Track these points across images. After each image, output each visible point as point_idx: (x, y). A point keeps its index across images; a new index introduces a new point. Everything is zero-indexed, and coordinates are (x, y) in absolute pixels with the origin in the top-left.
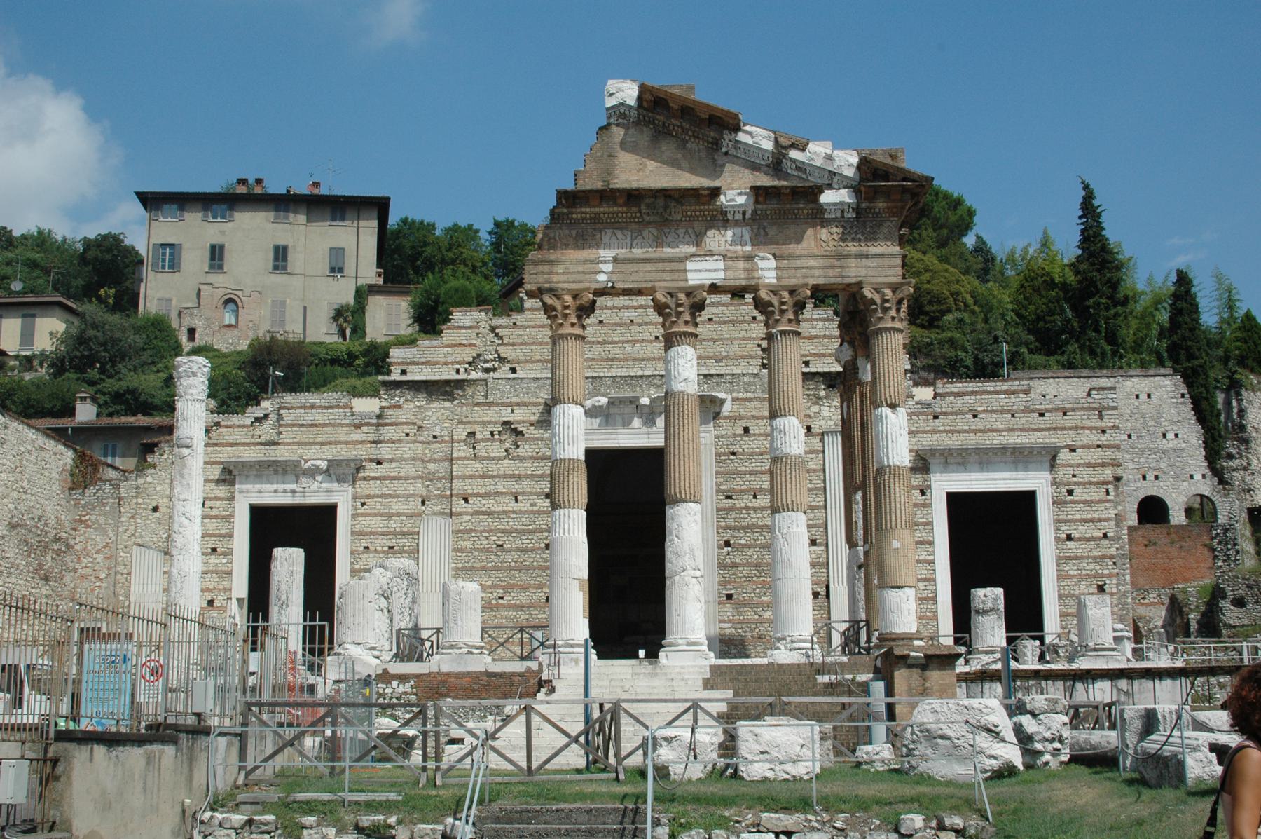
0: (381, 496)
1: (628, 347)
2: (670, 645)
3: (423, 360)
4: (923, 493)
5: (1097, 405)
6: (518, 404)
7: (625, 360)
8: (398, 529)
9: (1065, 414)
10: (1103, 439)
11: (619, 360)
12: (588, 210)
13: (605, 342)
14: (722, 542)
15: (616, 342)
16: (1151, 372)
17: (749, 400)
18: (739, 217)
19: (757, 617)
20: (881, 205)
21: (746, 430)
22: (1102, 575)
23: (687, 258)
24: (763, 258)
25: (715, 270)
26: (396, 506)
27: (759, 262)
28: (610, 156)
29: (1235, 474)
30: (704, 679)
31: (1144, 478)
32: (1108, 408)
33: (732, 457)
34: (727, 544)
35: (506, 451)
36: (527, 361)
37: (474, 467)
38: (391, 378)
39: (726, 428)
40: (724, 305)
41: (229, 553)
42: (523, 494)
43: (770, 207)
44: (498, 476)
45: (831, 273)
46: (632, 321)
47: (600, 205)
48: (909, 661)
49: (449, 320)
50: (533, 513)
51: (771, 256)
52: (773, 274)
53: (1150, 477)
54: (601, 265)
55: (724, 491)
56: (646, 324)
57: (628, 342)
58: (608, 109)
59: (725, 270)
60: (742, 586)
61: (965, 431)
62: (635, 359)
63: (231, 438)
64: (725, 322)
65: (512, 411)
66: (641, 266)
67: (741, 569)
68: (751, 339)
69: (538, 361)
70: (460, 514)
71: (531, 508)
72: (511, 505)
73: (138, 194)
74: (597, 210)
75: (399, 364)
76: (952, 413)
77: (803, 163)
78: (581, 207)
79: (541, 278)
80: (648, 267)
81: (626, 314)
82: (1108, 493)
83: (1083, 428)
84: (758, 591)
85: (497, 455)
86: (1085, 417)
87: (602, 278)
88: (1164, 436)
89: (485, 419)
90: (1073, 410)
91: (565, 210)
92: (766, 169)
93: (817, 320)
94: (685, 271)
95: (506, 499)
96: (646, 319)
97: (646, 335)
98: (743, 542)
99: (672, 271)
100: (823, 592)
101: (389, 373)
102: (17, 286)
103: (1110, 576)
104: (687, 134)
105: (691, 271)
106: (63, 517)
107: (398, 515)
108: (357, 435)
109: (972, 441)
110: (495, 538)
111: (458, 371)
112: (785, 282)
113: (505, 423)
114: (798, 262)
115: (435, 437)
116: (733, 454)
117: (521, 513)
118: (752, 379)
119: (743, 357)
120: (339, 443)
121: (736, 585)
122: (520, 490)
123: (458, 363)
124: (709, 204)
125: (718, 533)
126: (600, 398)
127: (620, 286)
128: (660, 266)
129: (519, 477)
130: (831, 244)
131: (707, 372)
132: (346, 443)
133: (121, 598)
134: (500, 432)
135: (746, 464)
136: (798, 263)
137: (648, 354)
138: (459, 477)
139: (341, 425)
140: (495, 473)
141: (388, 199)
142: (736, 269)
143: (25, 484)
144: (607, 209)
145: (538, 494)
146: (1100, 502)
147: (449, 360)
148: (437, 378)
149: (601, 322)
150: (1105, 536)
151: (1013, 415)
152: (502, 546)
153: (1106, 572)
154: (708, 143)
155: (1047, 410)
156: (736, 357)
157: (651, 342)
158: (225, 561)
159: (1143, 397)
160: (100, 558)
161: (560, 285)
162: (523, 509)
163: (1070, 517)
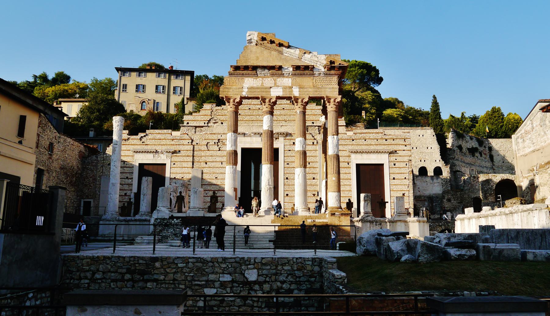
0: (180, 162)
3: (193, 120)
4: (348, 164)
7: (257, 121)
8: (185, 172)
9: (394, 140)
11: (255, 121)
12: (240, 72)
13: (250, 115)
14: (285, 178)
15: (254, 115)
16: (424, 128)
20: (333, 72)
22: (404, 191)
23: (270, 88)
25: (280, 92)
26: (185, 165)
29: (450, 160)
30: (272, 220)
31: (421, 161)
32: (407, 139)
34: (287, 178)
35: (219, 148)
37: (208, 153)
38: (184, 125)
39: (288, 142)
40: (288, 104)
41: (132, 178)
46: (259, 109)
49: (203, 107)
52: (298, 93)
53: (423, 161)
55: (286, 162)
57: (258, 115)
58: (248, 40)
61: (362, 145)
63: (133, 143)
64: (289, 110)
65: (221, 136)
66: (256, 90)
70: (204, 168)
72: (220, 165)
73: (115, 68)
74: (243, 72)
75: (187, 121)
76: (358, 139)
79: (225, 93)
80: (259, 90)
82: (406, 165)
83: (400, 145)
85: (216, 149)
88: (427, 148)
89: (213, 138)
91: (233, 72)
93: (317, 109)
94: (270, 92)
99: (266, 92)
100: (317, 194)
101: (183, 123)
102: (78, 96)
103: (407, 190)
106: (80, 166)
107: (185, 167)
108: (173, 143)
109: (364, 148)
111: (205, 123)
112: (301, 96)
113: (219, 140)
115: (197, 144)
120: (167, 145)
123: (205, 121)
127: (249, 96)
128: (263, 90)
132: (169, 145)
133: (97, 192)
138: (204, 156)
139: (168, 139)
141: (194, 72)
143: (66, 156)
146: (404, 167)
147: (202, 120)
148: (198, 125)
149: (250, 109)
150: (405, 178)
151: (377, 140)
153: (406, 189)
155: (389, 139)
158: (130, 181)
159: (421, 136)
160: (91, 179)
161: (231, 96)
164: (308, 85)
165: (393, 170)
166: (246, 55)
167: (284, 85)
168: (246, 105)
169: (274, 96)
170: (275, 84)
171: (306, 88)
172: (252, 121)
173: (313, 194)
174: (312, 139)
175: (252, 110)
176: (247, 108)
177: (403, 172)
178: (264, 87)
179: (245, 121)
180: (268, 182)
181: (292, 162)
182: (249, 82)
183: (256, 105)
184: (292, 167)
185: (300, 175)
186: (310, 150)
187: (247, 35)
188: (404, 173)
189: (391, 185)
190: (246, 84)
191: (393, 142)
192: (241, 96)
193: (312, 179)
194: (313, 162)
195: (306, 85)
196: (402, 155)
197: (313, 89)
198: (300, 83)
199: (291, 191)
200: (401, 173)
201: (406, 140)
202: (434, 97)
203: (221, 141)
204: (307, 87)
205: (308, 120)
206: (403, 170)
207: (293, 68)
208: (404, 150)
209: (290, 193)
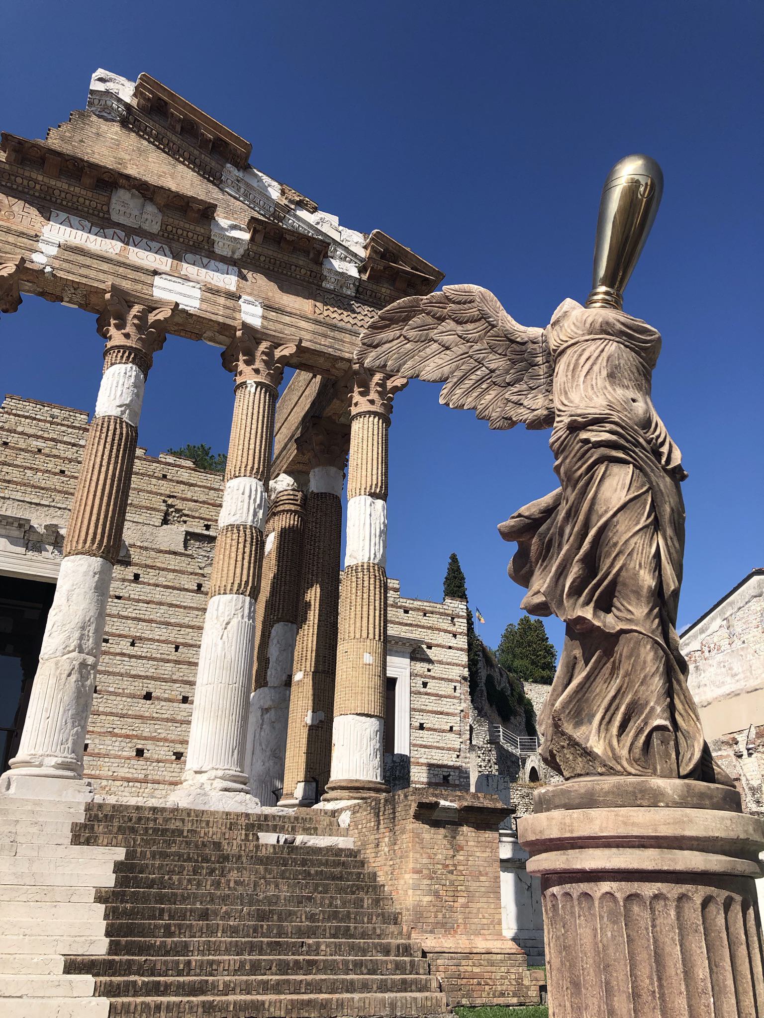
1: (29, 473)
2: (27, 763)
5: (450, 612)
7: (25, 485)
10: (455, 642)
11: (17, 483)
12: (40, 178)
17: (146, 549)
21: (137, 577)
23: (155, 273)
24: (249, 303)
28: (82, 141)
33: (116, 600)
43: (266, 251)
48: (436, 815)
56: (55, 456)
59: (202, 300)
62: (33, 486)
66: (95, 263)
68: (157, 494)
74: (53, 182)
80: (105, 266)
81: (35, 443)
82: (455, 689)
83: (439, 630)
86: (441, 620)
87: (39, 260)
90: (432, 613)
91: (7, 167)
94: (152, 285)
96: (55, 452)
97: (50, 466)
99: (135, 281)
105: (159, 288)
119: (148, 508)
128: (121, 270)
137: (49, 484)
142: (215, 303)
144: (65, 186)
155: (412, 609)
156: (141, 507)
157: (55, 474)
163: (423, 707)
165: (422, 702)
166: (77, 138)
173: (175, 754)
174: (196, 574)
175: (13, 448)
177: (446, 710)
178: (127, 262)
180: (77, 635)
181: (120, 636)
183: (29, 436)
184: (118, 651)
185: (234, 622)
186: (185, 608)
187: (95, 76)
188: (448, 714)
189: (415, 745)
191: (424, 621)
192: (23, 260)
193: (177, 701)
194: (191, 646)
196: (445, 660)
197: (313, 325)
199: (100, 734)
200: (441, 713)
201: (456, 620)
202: (454, 558)
204: (294, 311)
205: (194, 517)
206: (446, 705)
208: (450, 648)
209: (97, 741)
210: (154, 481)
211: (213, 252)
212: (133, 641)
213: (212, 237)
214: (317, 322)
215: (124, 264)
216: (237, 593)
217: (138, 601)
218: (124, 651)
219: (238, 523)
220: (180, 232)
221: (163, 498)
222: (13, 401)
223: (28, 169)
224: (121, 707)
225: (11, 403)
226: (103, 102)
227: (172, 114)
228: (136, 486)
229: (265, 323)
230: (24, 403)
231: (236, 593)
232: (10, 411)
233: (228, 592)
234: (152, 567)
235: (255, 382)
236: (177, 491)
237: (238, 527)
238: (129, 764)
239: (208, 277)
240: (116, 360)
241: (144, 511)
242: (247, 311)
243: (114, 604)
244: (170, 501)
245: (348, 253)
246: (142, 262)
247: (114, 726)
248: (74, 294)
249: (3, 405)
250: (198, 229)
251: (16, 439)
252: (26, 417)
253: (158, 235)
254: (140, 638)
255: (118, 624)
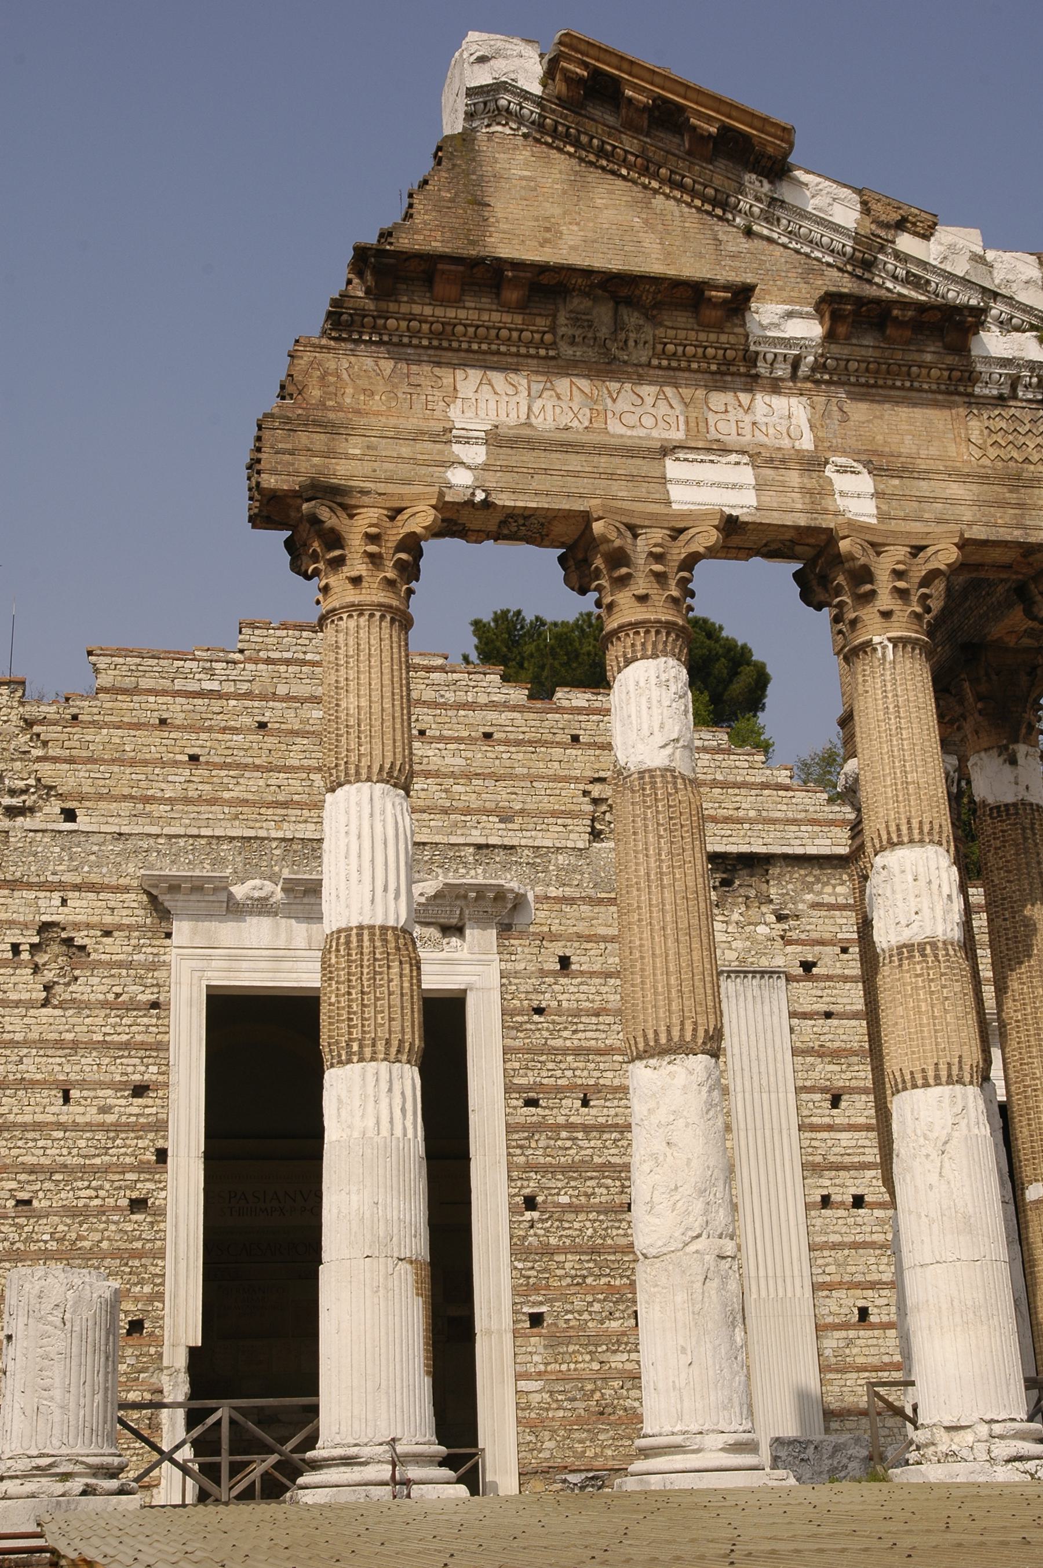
6: (77, 888)
11: (300, 805)
12: (428, 311)
13: (270, 768)
14: (519, 1200)
17: (570, 901)
18: (782, 371)
19: (596, 1366)
21: (565, 962)
23: (666, 450)
24: (842, 470)
25: (734, 486)
27: (835, 477)
33: (536, 1018)
34: (530, 1203)
35: (47, 988)
36: (101, 797)
40: (514, 708)
42: (82, 1084)
44: (26, 1043)
45: (1005, 516)
47: (456, 302)
50: (103, 1127)
51: (860, 467)
54: (456, 448)
55: (520, 1089)
58: (471, 92)
60: (564, 1298)
64: (518, 743)
65: (64, 902)
66: (555, 460)
67: (562, 1258)
68: (566, 779)
69: (125, 798)
71: (100, 1118)
72: (55, 1110)
74: (451, 313)
77: (923, 264)
78: (411, 301)
80: (575, 463)
84: (597, 1307)
85: (25, 996)
87: (460, 478)
91: (370, 305)
92: (836, 273)
94: (663, 480)
95: (43, 1096)
98: (564, 1199)
99: (632, 478)
104: (656, 176)
105: (679, 482)
110: (13, 1185)
113: (45, 927)
114: (922, 483)
116: (539, 1011)
117: (76, 1127)
118: (573, 860)
119: (554, 814)
121: (552, 1294)
122: (73, 1077)
124: (721, 330)
125: (510, 1179)
126: (257, 882)
129: (75, 1046)
130: (993, 453)
131: (482, 841)
134: (32, 945)
135: (565, 1034)
136: (924, 487)
140: (18, 1037)
142: (784, 487)
144: (473, 315)
145: (117, 1087)
149: (262, 725)
152: (28, 1202)
154: (705, 199)
156: (541, 814)
162: (80, 1119)
164: (933, 451)
167: (761, 438)
168: (238, 696)
169: (704, 515)
170: (696, 426)
171: (925, 475)
172: (277, 804)
176: (247, 721)
179: (230, 803)
182: (492, 398)
190: (469, 414)
192: (441, 494)
195: (923, 453)
197: (974, 487)
198: (879, 438)
203: (64, 935)
207: (836, 318)
210: (557, 752)
211: (757, 376)
212: (585, 1095)
213: (753, 348)
214: (983, 479)
215: (604, 446)
216: (950, 1082)
217: (577, 1013)
218: (572, 1119)
219: (918, 939)
220: (690, 350)
221: (581, 787)
222: (257, 632)
223: (405, 299)
224: (590, 1232)
225: (253, 639)
226: (492, 106)
227: (630, 100)
228: (525, 771)
229: (884, 507)
230: (279, 633)
231: (948, 1083)
232: (254, 655)
233: (931, 1081)
234: (589, 939)
235: (889, 639)
236: (604, 766)
237: (922, 947)
238: (626, 1344)
239: (757, 432)
240: (633, 652)
241: (551, 820)
242: (845, 489)
243: (533, 1027)
244: (596, 790)
245: (1012, 306)
246: (634, 433)
247: (585, 1272)
248: (524, 525)
249: (240, 646)
250: (723, 338)
251: (279, 713)
252: (288, 662)
253: (649, 365)
254: (598, 1089)
255: (550, 1066)
